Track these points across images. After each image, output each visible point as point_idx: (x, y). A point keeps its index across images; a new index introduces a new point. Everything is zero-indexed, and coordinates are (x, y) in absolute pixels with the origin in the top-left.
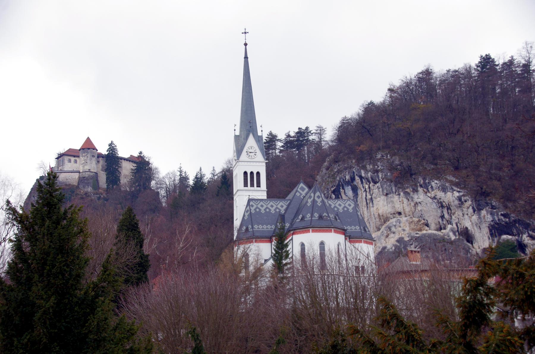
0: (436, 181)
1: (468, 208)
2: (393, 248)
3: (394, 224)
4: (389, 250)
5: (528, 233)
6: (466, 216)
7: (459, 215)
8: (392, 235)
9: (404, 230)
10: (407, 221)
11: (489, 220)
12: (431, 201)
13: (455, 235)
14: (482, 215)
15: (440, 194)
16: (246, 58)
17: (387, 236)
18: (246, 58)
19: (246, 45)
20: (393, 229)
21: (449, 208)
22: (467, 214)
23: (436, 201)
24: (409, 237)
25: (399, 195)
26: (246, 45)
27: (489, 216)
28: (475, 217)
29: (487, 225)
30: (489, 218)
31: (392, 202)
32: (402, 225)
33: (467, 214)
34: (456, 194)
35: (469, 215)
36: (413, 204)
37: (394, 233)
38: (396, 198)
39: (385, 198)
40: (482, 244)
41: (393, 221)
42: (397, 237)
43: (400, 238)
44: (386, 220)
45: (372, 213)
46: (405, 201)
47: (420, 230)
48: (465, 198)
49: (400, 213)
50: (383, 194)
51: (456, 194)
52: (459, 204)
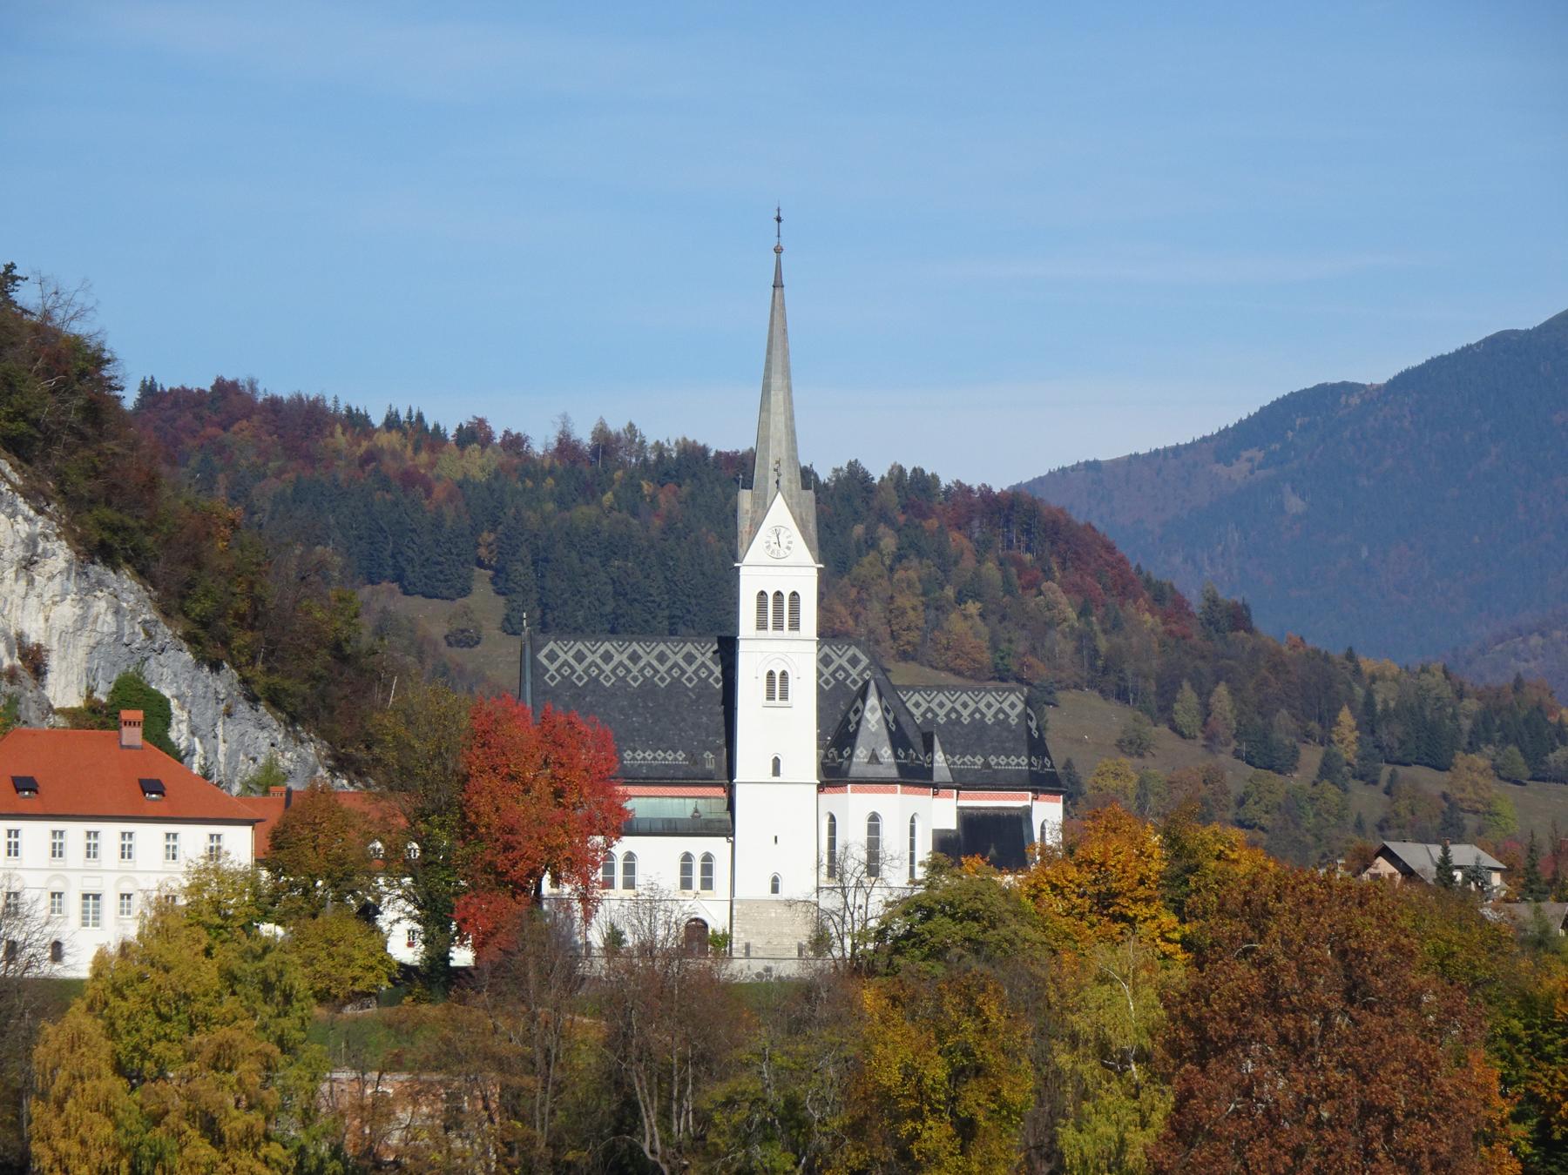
1: (51, 578)
5: (178, 688)
6: (33, 601)
7: (13, 592)
11: (105, 629)
13: (11, 654)
14: (94, 611)
16: (778, 285)
18: (778, 285)
19: (778, 250)
22: (40, 596)
26: (778, 250)
27: (110, 618)
28: (67, 612)
29: (92, 642)
30: (107, 623)
33: (40, 596)
34: (23, 528)
35: (47, 596)
40: (59, 695)
48: (49, 546)
51: (23, 528)
52: (24, 558)
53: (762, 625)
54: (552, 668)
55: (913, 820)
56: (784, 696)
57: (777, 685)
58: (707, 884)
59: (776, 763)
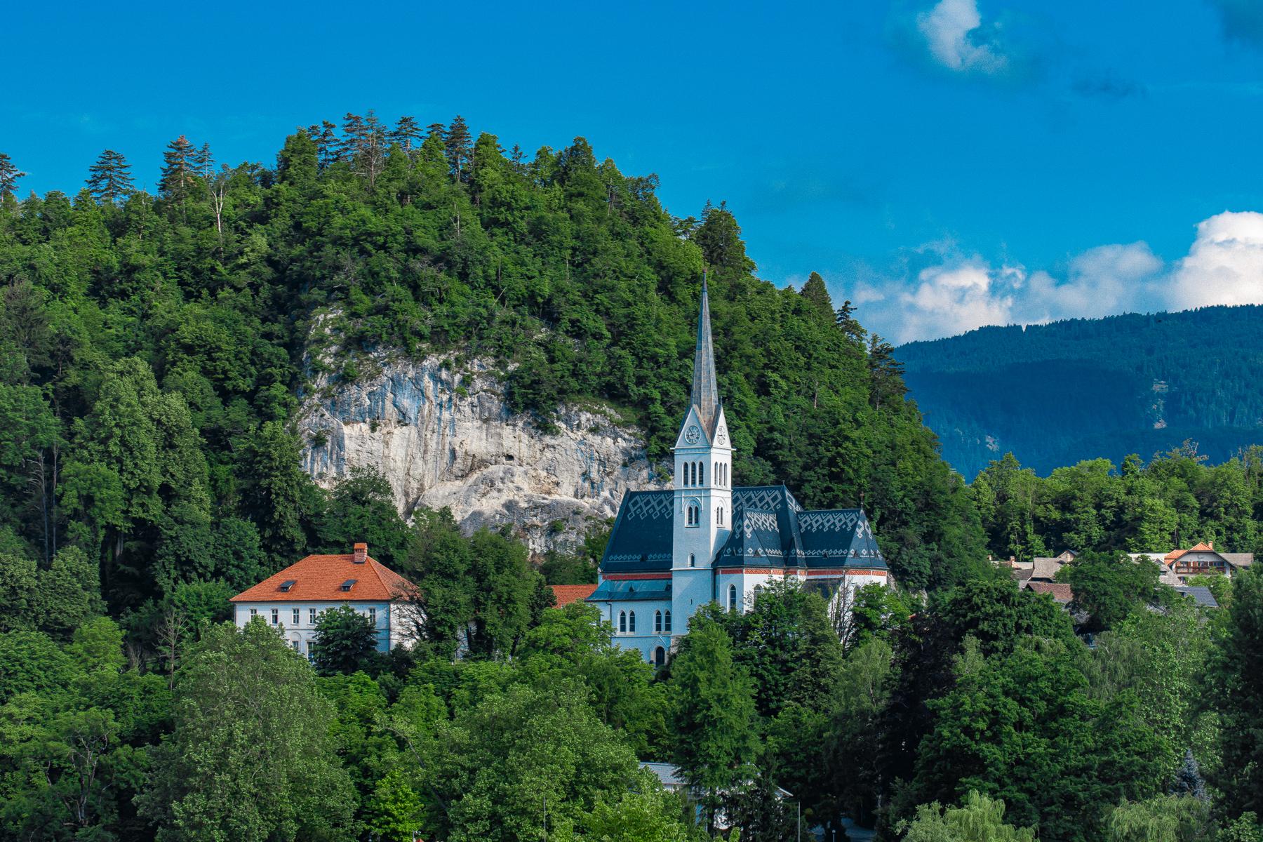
0: (589, 415)
2: (498, 517)
3: (501, 474)
4: (486, 520)
8: (495, 493)
9: (518, 489)
10: (526, 473)
12: (574, 446)
15: (595, 440)
17: (484, 495)
20: (499, 484)
21: (602, 463)
23: (583, 447)
24: (528, 502)
25: (515, 425)
31: (500, 436)
32: (516, 479)
36: (539, 446)
37: (499, 491)
38: (507, 431)
39: (485, 426)
41: (496, 470)
42: (505, 498)
43: (510, 502)
44: (484, 463)
45: (447, 447)
46: (525, 437)
47: (549, 493)
49: (510, 457)
50: (480, 418)
53: (686, 483)
54: (633, 510)
55: (733, 588)
56: (697, 521)
57: (696, 515)
58: (668, 628)
59: (693, 558)
